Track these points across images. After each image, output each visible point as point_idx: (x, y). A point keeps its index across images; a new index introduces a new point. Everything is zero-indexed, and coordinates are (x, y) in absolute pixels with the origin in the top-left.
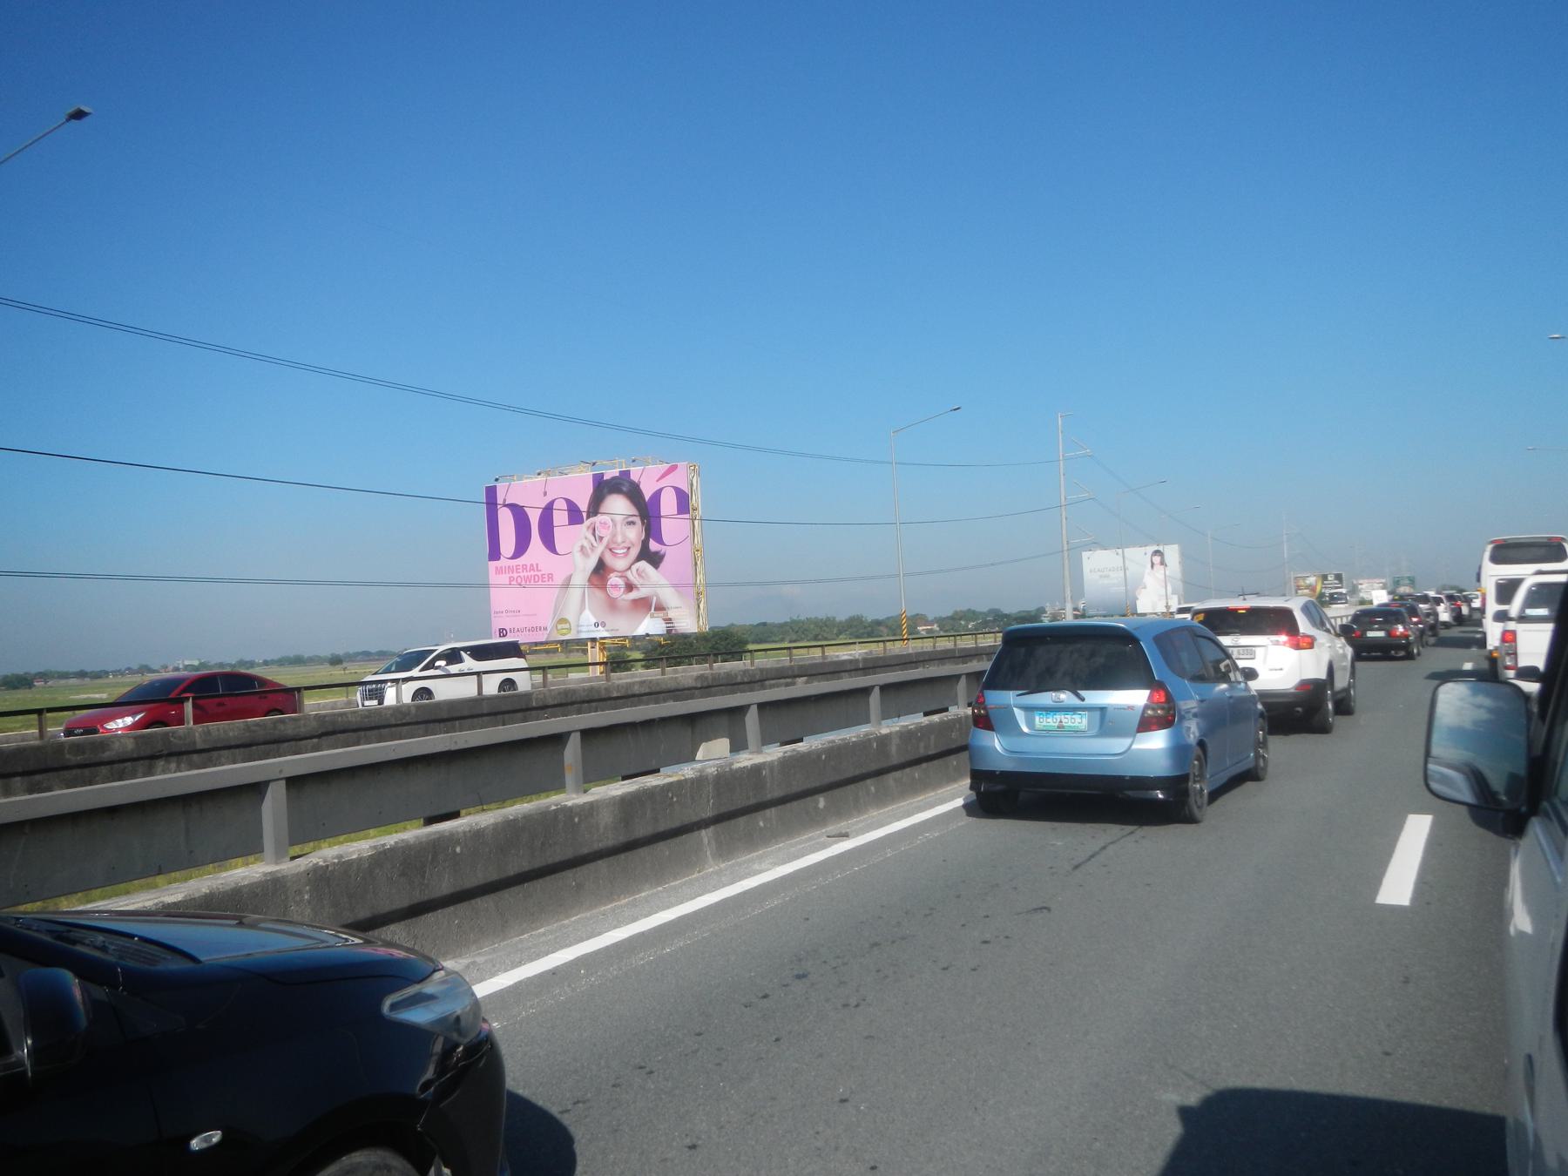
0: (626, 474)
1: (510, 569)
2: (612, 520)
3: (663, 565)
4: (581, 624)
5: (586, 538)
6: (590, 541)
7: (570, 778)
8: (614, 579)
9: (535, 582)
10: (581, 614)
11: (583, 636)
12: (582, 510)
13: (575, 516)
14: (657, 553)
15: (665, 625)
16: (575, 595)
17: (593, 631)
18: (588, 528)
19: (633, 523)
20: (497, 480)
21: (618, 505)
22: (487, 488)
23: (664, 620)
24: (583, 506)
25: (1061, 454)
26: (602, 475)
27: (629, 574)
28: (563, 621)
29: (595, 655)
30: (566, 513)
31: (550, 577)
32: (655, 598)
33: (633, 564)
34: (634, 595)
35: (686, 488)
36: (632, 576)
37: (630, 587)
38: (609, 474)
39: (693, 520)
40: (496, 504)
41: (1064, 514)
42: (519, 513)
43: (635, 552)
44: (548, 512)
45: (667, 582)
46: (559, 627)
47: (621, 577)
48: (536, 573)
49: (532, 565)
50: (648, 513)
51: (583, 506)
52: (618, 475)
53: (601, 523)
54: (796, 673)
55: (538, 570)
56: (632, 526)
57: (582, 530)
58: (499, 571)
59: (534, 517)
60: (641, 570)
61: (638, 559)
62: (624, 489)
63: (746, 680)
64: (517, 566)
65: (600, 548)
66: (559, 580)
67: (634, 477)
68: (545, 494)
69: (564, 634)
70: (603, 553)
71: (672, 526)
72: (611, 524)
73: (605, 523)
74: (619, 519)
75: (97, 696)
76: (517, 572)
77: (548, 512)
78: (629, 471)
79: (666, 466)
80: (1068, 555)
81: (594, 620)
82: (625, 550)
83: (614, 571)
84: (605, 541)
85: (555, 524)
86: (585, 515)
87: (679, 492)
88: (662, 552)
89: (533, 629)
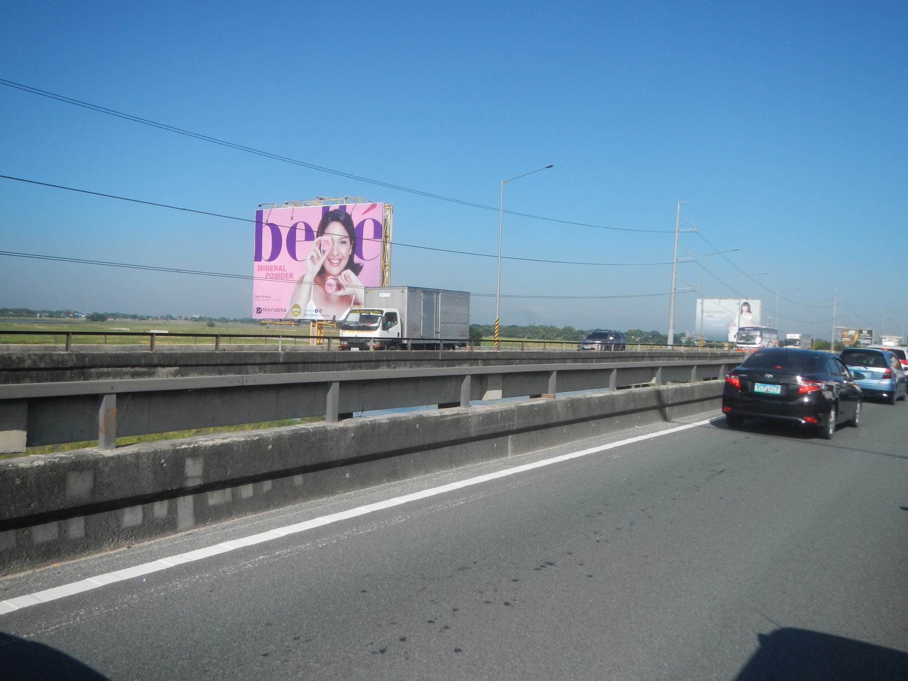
0: (343, 208)
1: (267, 268)
2: (332, 239)
3: (361, 273)
4: (307, 309)
5: (315, 251)
8: (330, 280)
9: (281, 278)
10: (308, 302)
11: (308, 318)
12: (314, 230)
13: (309, 236)
14: (358, 265)
16: (305, 288)
17: (314, 315)
18: (317, 243)
19: (344, 242)
20: (260, 206)
21: (336, 229)
22: (257, 211)
24: (315, 228)
25: (677, 229)
26: (328, 208)
27: (339, 278)
28: (297, 306)
29: (314, 331)
30: (304, 231)
31: (291, 275)
32: (354, 296)
33: (343, 271)
34: (341, 293)
35: (380, 221)
36: (341, 279)
37: (339, 287)
38: (334, 207)
39: (385, 243)
40: (262, 223)
41: (674, 269)
42: (275, 229)
43: (344, 263)
44: (293, 229)
45: (360, 284)
46: (294, 310)
47: (334, 279)
49: (280, 266)
50: (355, 236)
51: (315, 228)
52: (338, 208)
53: (324, 241)
54: (156, 361)
55: (284, 271)
56: (344, 245)
57: (313, 244)
58: (260, 268)
61: (346, 268)
62: (341, 218)
63: (42, 365)
64: (271, 266)
65: (323, 258)
66: (296, 278)
67: (348, 211)
68: (292, 218)
69: (296, 316)
70: (324, 262)
71: (370, 247)
72: (331, 242)
73: (327, 241)
74: (337, 238)
75: (118, 328)
76: (271, 270)
77: (293, 229)
79: (370, 204)
80: (674, 298)
81: (315, 308)
82: (338, 261)
83: (330, 275)
84: (327, 253)
86: (315, 234)
87: (376, 223)
89: (277, 310)
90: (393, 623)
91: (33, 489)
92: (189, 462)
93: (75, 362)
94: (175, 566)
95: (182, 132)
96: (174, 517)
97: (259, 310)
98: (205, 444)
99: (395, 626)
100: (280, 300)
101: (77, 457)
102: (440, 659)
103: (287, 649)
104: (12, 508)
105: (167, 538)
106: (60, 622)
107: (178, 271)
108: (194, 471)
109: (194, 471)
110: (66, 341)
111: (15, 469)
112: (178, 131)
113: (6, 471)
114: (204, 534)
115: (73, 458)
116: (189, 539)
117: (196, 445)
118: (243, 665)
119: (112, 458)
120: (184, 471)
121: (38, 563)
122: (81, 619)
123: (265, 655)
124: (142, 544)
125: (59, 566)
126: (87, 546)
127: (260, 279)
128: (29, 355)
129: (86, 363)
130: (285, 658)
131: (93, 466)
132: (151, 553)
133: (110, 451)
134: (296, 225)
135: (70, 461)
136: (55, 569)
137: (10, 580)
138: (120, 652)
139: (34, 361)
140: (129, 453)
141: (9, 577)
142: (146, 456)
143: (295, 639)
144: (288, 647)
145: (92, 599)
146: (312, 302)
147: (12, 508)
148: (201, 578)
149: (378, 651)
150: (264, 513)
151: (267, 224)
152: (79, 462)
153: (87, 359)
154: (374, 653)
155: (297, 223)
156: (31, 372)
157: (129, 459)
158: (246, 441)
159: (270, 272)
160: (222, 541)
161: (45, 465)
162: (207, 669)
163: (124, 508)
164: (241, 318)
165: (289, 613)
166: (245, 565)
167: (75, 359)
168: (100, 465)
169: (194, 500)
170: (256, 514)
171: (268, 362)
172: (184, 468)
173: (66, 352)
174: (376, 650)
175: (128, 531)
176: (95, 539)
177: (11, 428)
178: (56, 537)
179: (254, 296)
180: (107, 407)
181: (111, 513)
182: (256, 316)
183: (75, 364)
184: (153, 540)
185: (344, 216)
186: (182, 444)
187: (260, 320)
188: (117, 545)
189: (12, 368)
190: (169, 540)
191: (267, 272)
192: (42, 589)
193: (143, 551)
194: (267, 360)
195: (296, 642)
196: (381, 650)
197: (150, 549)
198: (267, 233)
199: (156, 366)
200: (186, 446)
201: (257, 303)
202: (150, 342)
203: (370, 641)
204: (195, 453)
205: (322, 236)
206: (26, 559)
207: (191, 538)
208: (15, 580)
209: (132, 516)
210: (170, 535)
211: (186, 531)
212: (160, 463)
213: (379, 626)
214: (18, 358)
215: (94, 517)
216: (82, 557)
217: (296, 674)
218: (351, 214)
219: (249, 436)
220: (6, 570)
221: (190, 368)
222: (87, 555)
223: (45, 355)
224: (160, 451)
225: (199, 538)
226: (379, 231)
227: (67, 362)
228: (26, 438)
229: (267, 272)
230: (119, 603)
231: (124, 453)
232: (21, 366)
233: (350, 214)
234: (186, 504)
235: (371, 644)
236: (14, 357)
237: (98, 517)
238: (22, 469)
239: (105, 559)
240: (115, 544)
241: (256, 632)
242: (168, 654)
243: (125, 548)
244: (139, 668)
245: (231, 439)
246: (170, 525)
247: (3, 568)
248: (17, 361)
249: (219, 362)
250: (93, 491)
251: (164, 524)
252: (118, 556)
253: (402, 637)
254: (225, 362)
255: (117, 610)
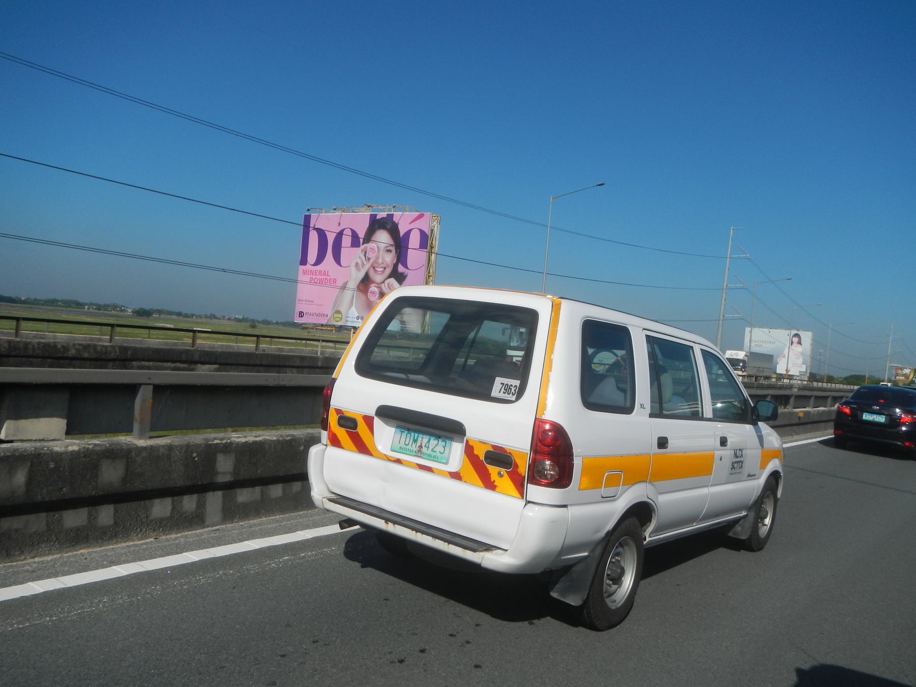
1: (312, 272)
4: (349, 315)
5: (360, 258)
6: (362, 260)
7: (136, 426)
8: (373, 288)
11: (349, 324)
13: (355, 242)
14: (402, 274)
15: (400, 325)
16: (348, 294)
17: (355, 322)
18: (362, 251)
19: (389, 251)
20: (308, 210)
21: (383, 237)
23: (400, 321)
24: (361, 234)
26: (376, 215)
27: (383, 285)
28: (338, 312)
31: (335, 281)
35: (428, 232)
36: (384, 287)
38: (381, 215)
39: (430, 253)
40: (309, 227)
42: (322, 234)
43: (388, 271)
44: (340, 235)
46: (336, 316)
47: (377, 287)
48: (327, 277)
49: (325, 271)
50: (400, 244)
51: (361, 234)
53: (370, 248)
54: (196, 358)
55: (328, 276)
56: (389, 253)
57: (358, 251)
58: (305, 272)
59: (331, 238)
60: (390, 284)
61: (390, 277)
62: (388, 227)
63: (86, 355)
64: (316, 271)
65: (368, 266)
66: (340, 283)
67: (395, 219)
68: (339, 224)
69: (337, 321)
70: (368, 270)
71: (415, 256)
74: (382, 246)
76: (316, 275)
77: (340, 235)
78: (393, 214)
79: (418, 213)
80: (723, 325)
82: (382, 269)
83: (373, 282)
84: (371, 261)
85: (342, 246)
86: (361, 241)
88: (405, 274)
90: (413, 634)
91: (67, 474)
92: (220, 458)
93: (118, 354)
94: (200, 561)
95: (235, 133)
96: (202, 512)
97: (301, 314)
98: (237, 440)
99: (415, 637)
100: (322, 305)
101: (111, 445)
102: (459, 673)
103: (304, 651)
104: (45, 491)
105: (194, 532)
106: (83, 608)
107: (224, 271)
108: (225, 467)
109: (225, 467)
110: (110, 334)
111: (50, 453)
112: (233, 132)
113: (40, 455)
114: (231, 531)
115: (107, 445)
116: (215, 535)
117: (229, 441)
118: (259, 664)
119: (145, 448)
120: (215, 466)
121: (66, 548)
122: (104, 606)
123: (283, 656)
124: (169, 536)
125: (86, 552)
126: (116, 535)
127: (303, 282)
128: (74, 345)
129: (128, 355)
130: (303, 661)
131: (126, 455)
132: (177, 545)
133: (143, 441)
134: (343, 230)
135: (103, 448)
136: (82, 555)
137: (38, 563)
138: (139, 641)
139: (78, 350)
140: (162, 444)
141: (37, 559)
142: (178, 449)
143: (314, 642)
144: (306, 649)
145: (116, 587)
146: (353, 308)
147: (45, 491)
148: (225, 574)
149: (396, 661)
150: (292, 514)
151: (314, 229)
152: (113, 450)
153: (129, 352)
154: (392, 662)
155: (344, 229)
156: (74, 362)
157: (162, 450)
158: (278, 441)
159: (314, 277)
160: (247, 539)
161: (79, 451)
162: (224, 665)
163: (154, 499)
164: (283, 321)
165: (310, 616)
166: (269, 564)
167: (118, 351)
168: (133, 454)
169: (224, 496)
170: (284, 514)
171: (307, 365)
172: (215, 463)
173: (109, 344)
174: (394, 660)
175: (156, 523)
176: (123, 527)
177: (52, 415)
178: (85, 523)
179: (297, 300)
180: (143, 398)
181: (141, 504)
182: (298, 320)
183: (118, 356)
184: (180, 532)
185: (391, 224)
186: (215, 439)
187: (302, 324)
188: (144, 535)
189: (56, 356)
190: (196, 534)
191: (311, 276)
192: (68, 573)
193: (170, 543)
194: (306, 364)
195: (315, 645)
196: (400, 660)
197: (177, 542)
198: (314, 238)
199: (196, 363)
200: (218, 441)
201: (300, 307)
202: (191, 340)
203: (389, 650)
204: (227, 448)
205: (368, 243)
206: (55, 543)
207: (217, 534)
208: (42, 562)
209: (161, 508)
210: (197, 530)
211: (213, 526)
212: (192, 457)
213: (399, 635)
214: (63, 347)
215: (124, 506)
216: (109, 544)
217: (312, 677)
218: (398, 223)
219: (281, 436)
220: (35, 552)
221: (229, 367)
222: (114, 543)
223: (89, 345)
224: (193, 445)
225: (225, 534)
226: (425, 241)
227: (110, 353)
228: (66, 426)
229: (311, 276)
230: (143, 593)
231: (157, 444)
232: (65, 355)
233: (397, 222)
234: (215, 500)
235: (390, 653)
236: (59, 346)
237: (127, 507)
238: (57, 453)
239: (132, 549)
240: (143, 534)
241: (276, 632)
242: (186, 647)
243: (152, 539)
244: (157, 659)
245: (264, 437)
246: (197, 519)
247: (32, 550)
248: (62, 350)
249: (258, 363)
250: (124, 480)
251: (192, 518)
252: (145, 546)
253: (422, 649)
254: (264, 362)
255: (139, 600)
